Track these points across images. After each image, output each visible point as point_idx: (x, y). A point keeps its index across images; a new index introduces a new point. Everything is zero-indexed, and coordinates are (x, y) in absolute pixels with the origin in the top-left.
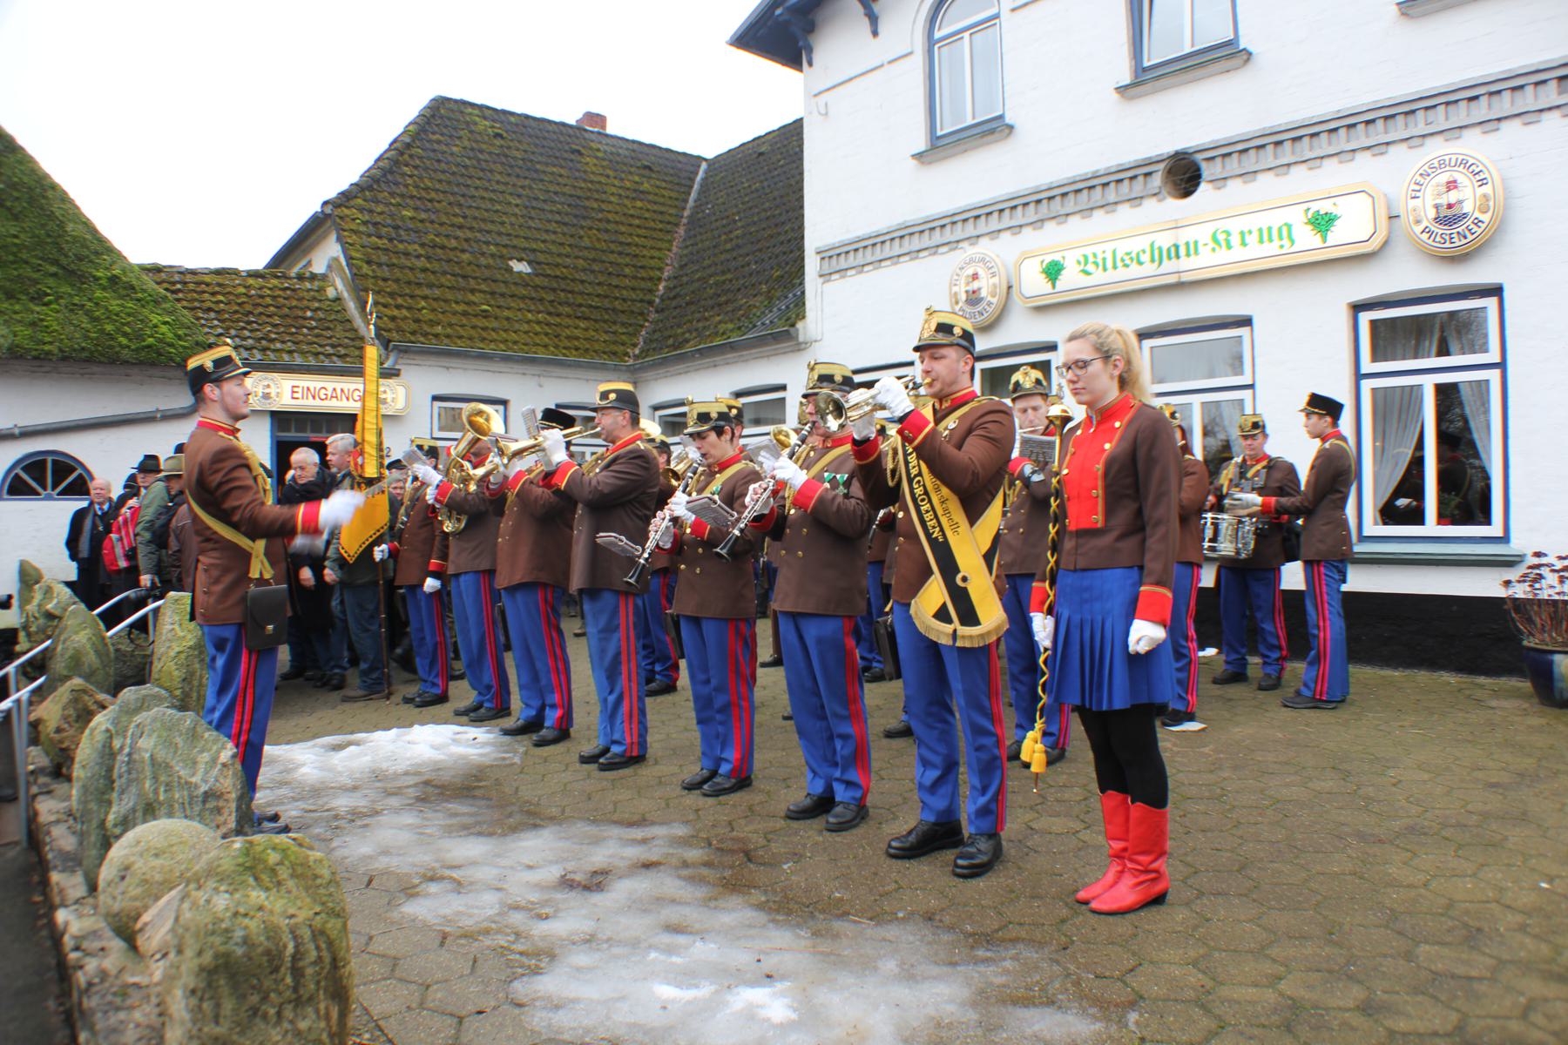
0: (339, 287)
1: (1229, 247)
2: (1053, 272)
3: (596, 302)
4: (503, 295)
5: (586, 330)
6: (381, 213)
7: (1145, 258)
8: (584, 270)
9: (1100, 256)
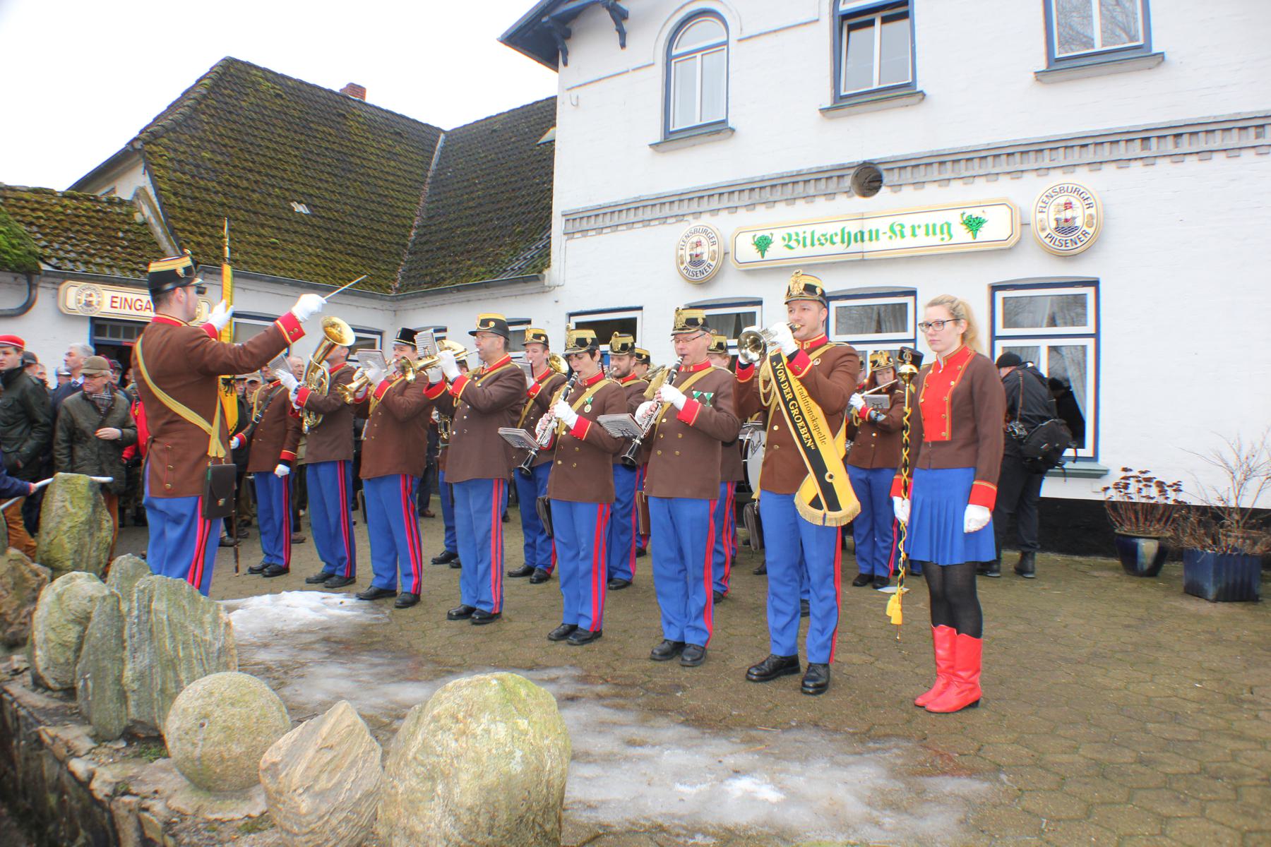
0: (145, 213)
1: (903, 236)
2: (763, 244)
3: (362, 242)
4: (287, 231)
5: (355, 265)
6: (183, 153)
7: (837, 239)
8: (351, 215)
9: (801, 236)
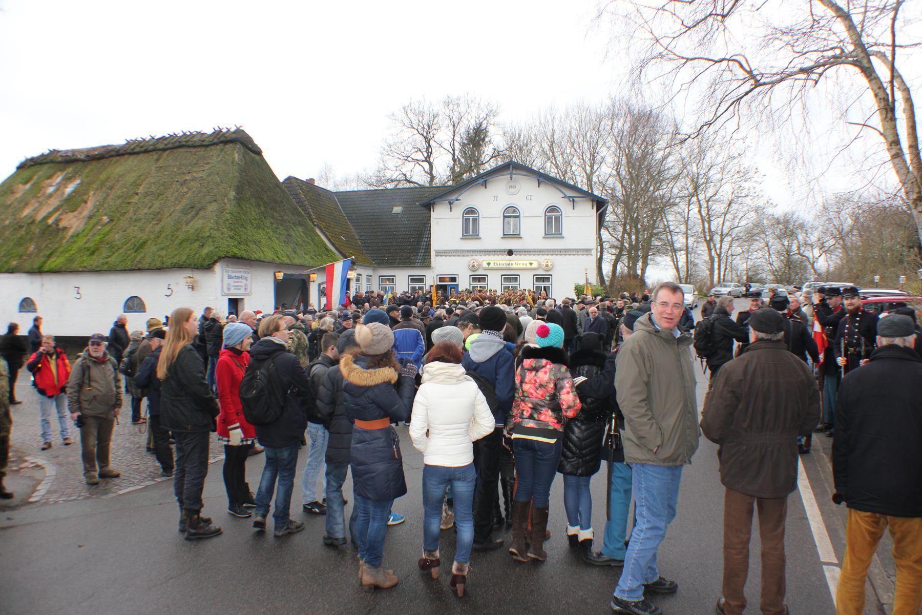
2: (489, 264)
